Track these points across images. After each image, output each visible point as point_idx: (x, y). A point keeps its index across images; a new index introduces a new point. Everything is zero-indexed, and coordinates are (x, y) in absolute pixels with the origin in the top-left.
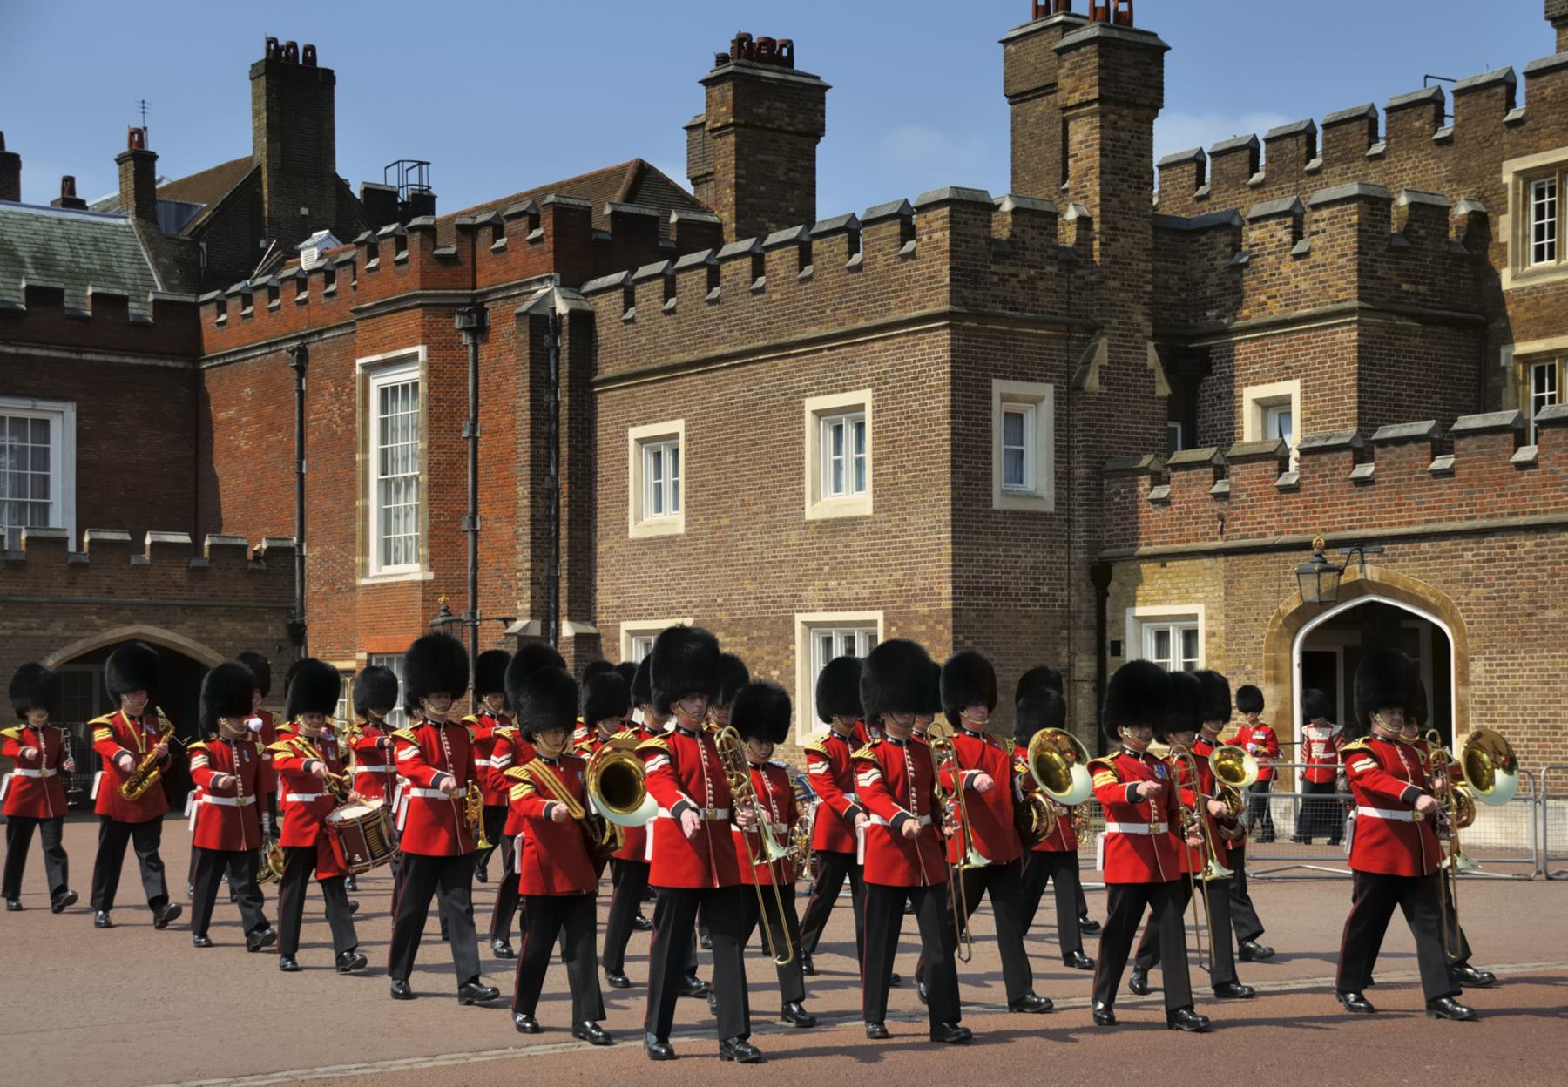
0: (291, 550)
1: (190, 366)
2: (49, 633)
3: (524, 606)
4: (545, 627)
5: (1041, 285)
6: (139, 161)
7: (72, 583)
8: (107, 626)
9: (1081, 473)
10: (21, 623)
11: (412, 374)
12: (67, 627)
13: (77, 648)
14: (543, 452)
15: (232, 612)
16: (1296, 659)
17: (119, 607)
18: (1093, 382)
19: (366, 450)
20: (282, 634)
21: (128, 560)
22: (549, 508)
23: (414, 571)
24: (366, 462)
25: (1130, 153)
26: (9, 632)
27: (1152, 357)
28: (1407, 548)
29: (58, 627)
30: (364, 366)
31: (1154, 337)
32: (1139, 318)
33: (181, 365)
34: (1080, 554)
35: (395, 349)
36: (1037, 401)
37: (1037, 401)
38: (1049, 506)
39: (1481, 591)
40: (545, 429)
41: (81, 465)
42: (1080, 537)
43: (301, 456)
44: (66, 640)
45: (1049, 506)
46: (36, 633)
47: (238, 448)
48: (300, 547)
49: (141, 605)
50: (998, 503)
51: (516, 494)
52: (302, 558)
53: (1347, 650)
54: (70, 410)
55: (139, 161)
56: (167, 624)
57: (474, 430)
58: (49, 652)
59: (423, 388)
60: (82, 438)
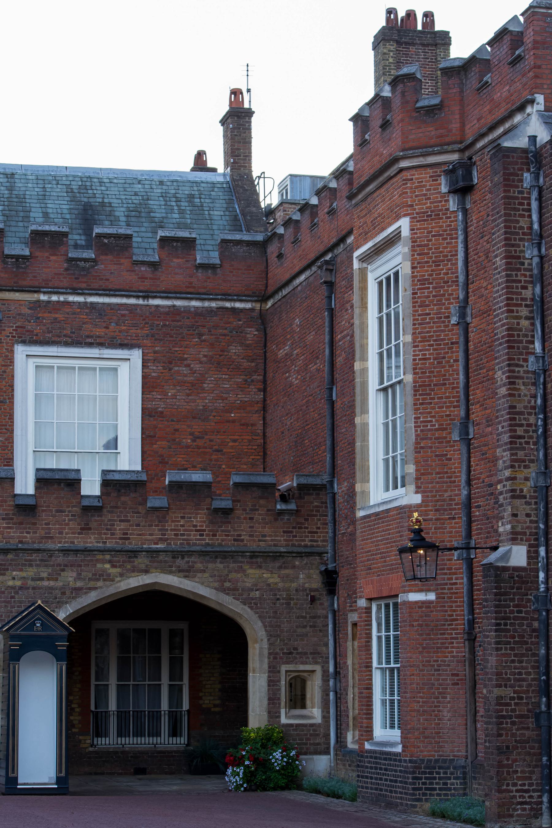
0: (322, 487)
1: (258, 306)
2: (60, 584)
3: (504, 528)
4: (532, 556)
6: (238, 121)
7: (86, 529)
8: (121, 575)
10: (30, 572)
11: (397, 260)
12: (79, 578)
13: (90, 599)
14: (525, 323)
15: (256, 557)
17: (134, 553)
19: (364, 358)
20: (316, 582)
21: (145, 501)
22: (535, 396)
23: (408, 497)
24: (365, 371)
26: (18, 583)
29: (69, 577)
30: (364, 259)
33: (248, 306)
35: (383, 229)
40: (527, 293)
41: (148, 413)
43: (332, 382)
44: (77, 592)
46: (46, 583)
47: (291, 384)
48: (331, 483)
49: (158, 551)
51: (492, 379)
52: (334, 494)
54: (136, 355)
55: (238, 121)
56: (187, 572)
57: (463, 315)
58: (60, 604)
59: (406, 270)
60: (148, 385)
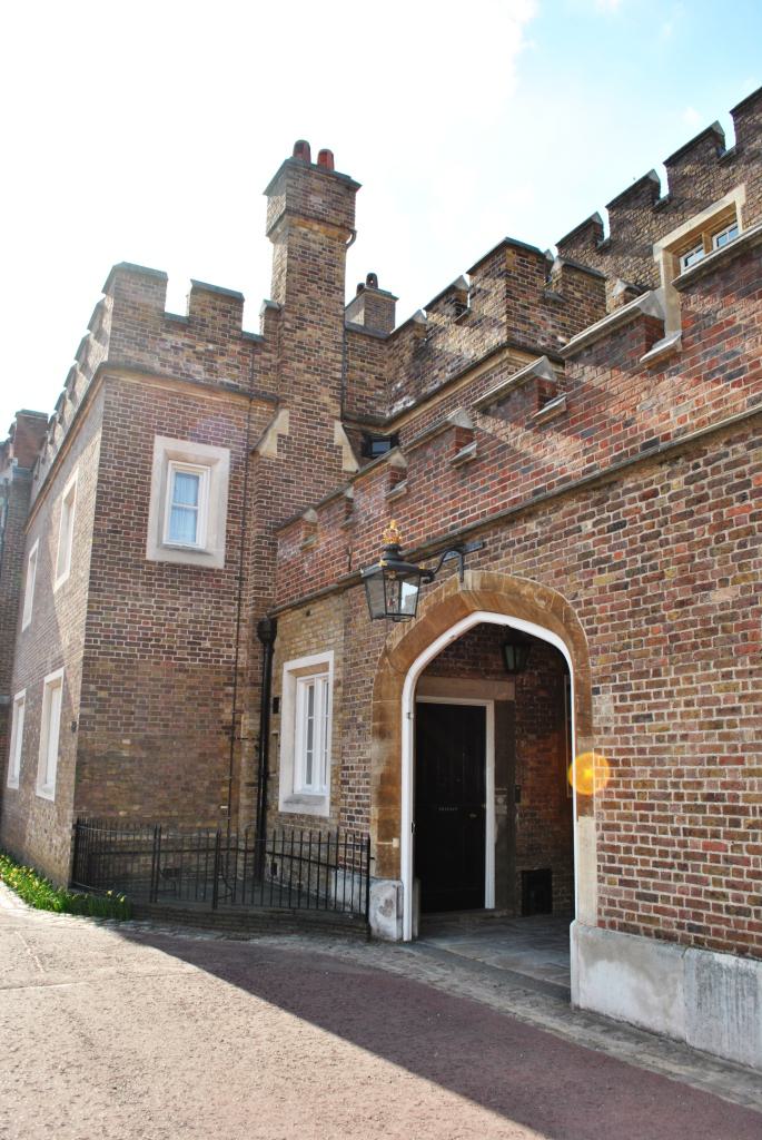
5: (221, 360)
9: (253, 533)
16: (407, 706)
18: (269, 447)
25: (321, 262)
27: (339, 434)
28: (509, 535)
31: (343, 418)
32: (327, 399)
34: (247, 612)
36: (210, 463)
37: (210, 463)
38: (218, 562)
39: (607, 578)
42: (249, 596)
45: (218, 562)
50: (152, 554)
53: (499, 706)
